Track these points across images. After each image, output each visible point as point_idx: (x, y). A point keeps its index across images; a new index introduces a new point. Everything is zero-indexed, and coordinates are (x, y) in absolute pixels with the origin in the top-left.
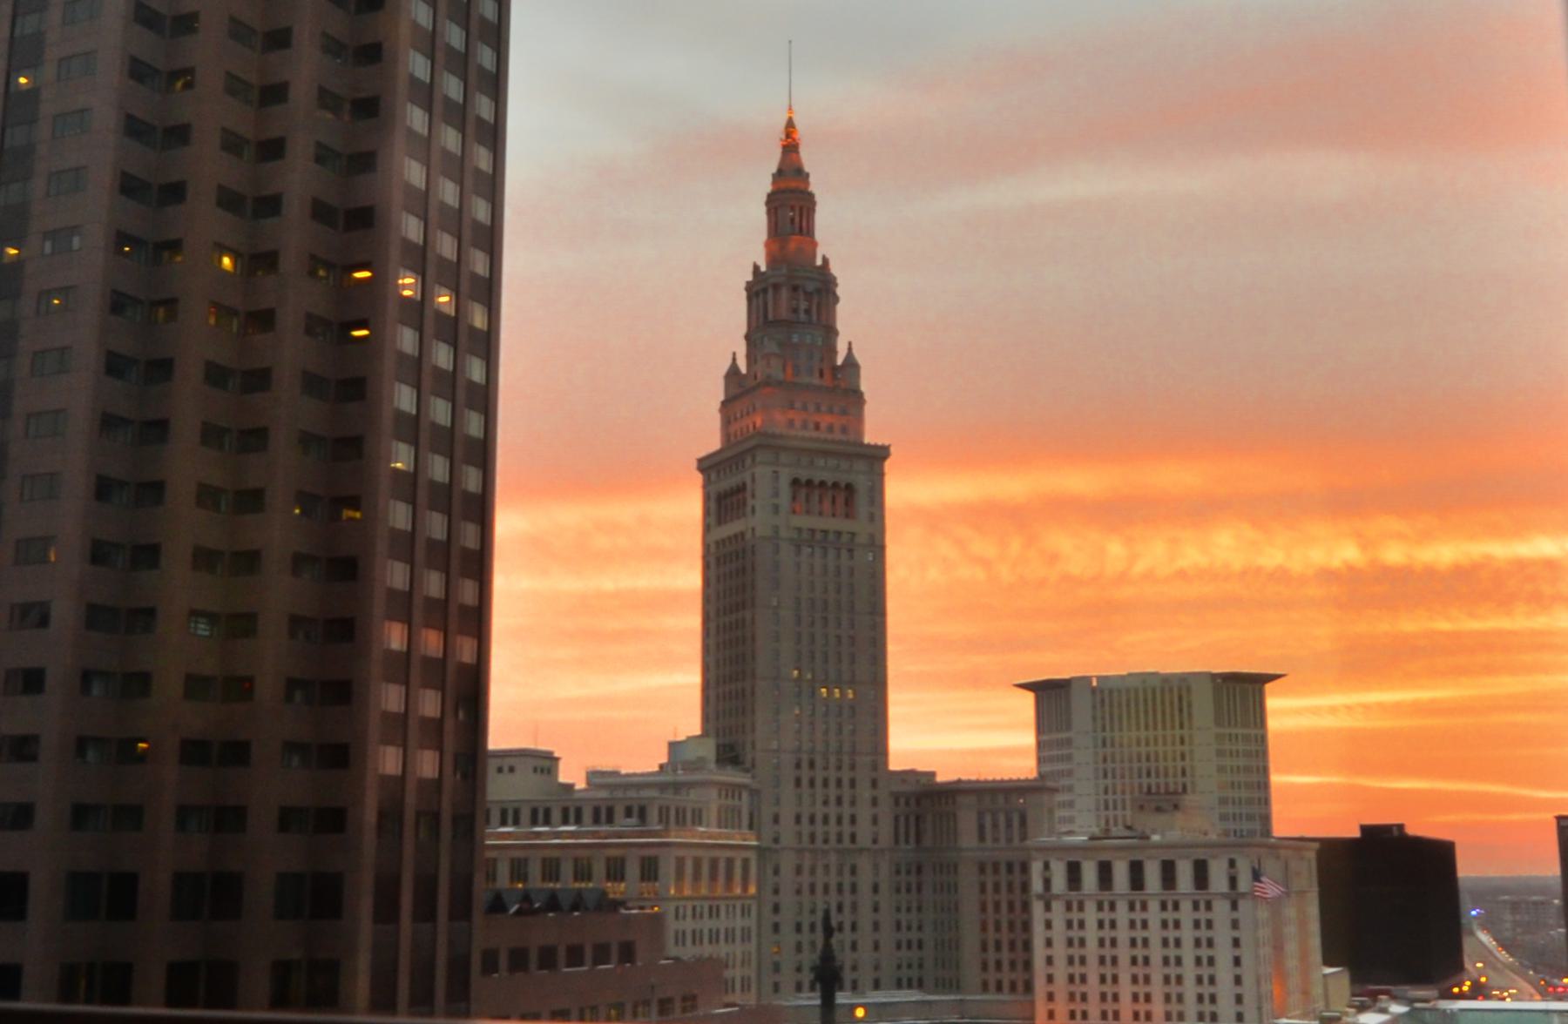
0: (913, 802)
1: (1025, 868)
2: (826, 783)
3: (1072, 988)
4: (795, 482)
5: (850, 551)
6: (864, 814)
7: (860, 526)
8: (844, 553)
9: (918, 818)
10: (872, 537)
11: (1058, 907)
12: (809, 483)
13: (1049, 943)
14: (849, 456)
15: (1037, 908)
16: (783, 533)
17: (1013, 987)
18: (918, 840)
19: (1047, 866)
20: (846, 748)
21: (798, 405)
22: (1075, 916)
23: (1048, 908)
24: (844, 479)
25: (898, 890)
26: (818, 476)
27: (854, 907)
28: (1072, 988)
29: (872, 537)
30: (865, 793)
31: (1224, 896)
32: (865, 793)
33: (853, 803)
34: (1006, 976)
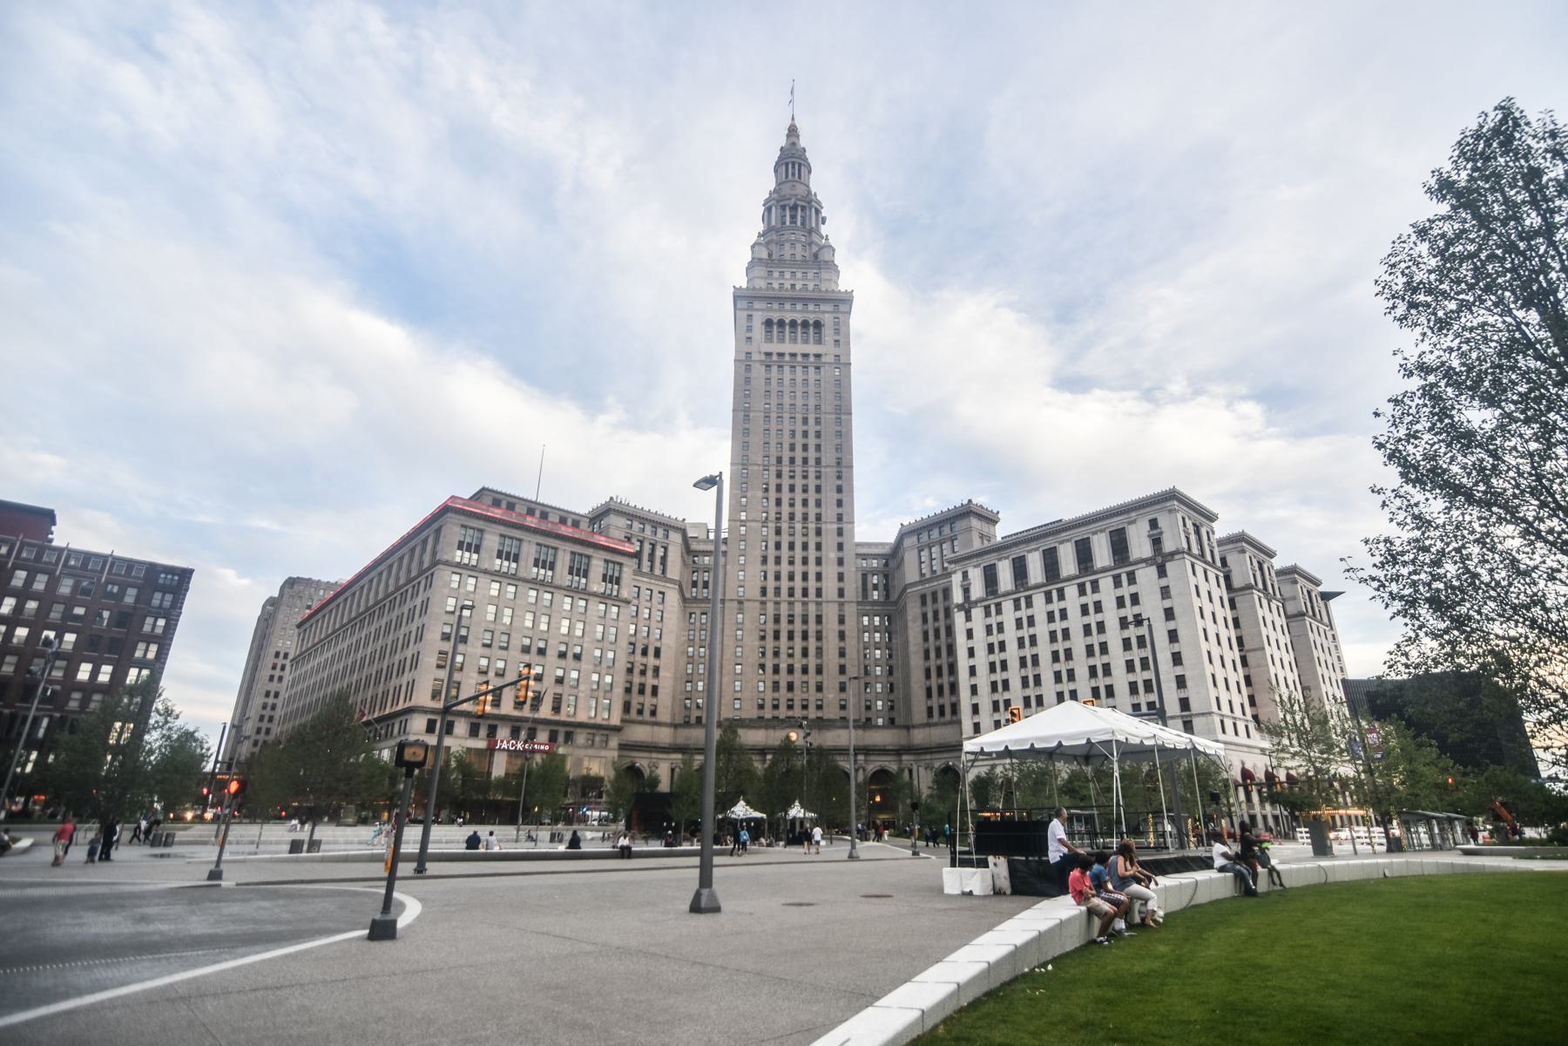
2: (792, 546)
3: (996, 697)
4: (768, 323)
6: (830, 571)
7: (827, 349)
8: (811, 370)
9: (886, 576)
11: (977, 613)
12: (781, 323)
13: (971, 653)
15: (959, 617)
16: (755, 357)
18: (887, 596)
19: (965, 575)
20: (812, 517)
21: (776, 274)
23: (968, 618)
24: (811, 318)
26: (788, 318)
27: (819, 651)
28: (996, 697)
30: (831, 555)
31: (1146, 561)
32: (831, 555)
34: (947, 700)
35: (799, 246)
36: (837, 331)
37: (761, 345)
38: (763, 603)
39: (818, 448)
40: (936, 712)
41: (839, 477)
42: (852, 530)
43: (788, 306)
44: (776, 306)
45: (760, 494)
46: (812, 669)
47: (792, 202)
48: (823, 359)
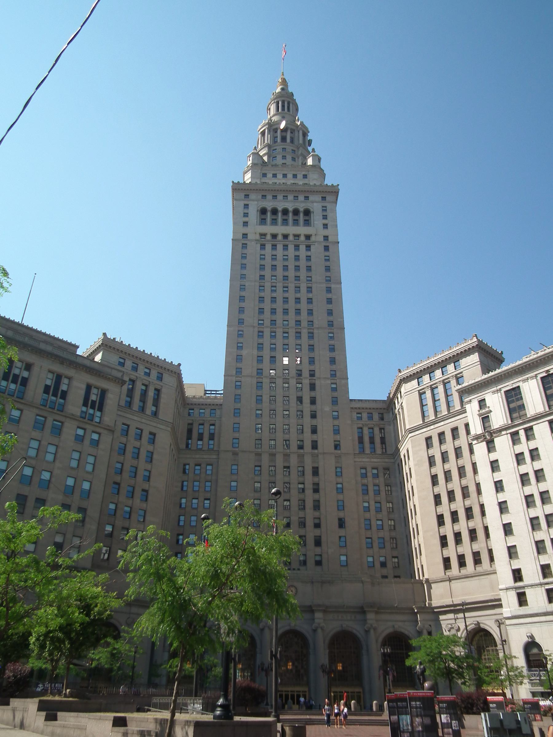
0: (376, 417)
1: (467, 425)
4: (263, 211)
5: (308, 247)
8: (303, 248)
10: (326, 238)
11: (503, 442)
14: (307, 193)
16: (250, 237)
17: (477, 560)
19: (482, 403)
22: (524, 447)
24: (301, 207)
25: (366, 492)
29: (326, 238)
30: (324, 407)
33: (314, 416)
35: (289, 158)
36: (325, 217)
37: (255, 229)
38: (259, 455)
39: (310, 312)
40: (454, 563)
41: (332, 338)
42: (346, 385)
43: (280, 197)
44: (269, 197)
45: (255, 352)
46: (310, 523)
47: (283, 125)
48: (313, 239)
